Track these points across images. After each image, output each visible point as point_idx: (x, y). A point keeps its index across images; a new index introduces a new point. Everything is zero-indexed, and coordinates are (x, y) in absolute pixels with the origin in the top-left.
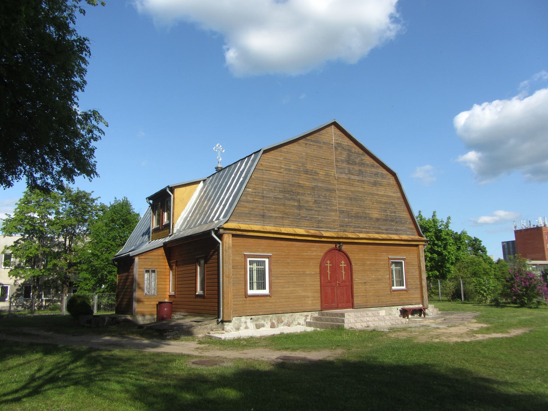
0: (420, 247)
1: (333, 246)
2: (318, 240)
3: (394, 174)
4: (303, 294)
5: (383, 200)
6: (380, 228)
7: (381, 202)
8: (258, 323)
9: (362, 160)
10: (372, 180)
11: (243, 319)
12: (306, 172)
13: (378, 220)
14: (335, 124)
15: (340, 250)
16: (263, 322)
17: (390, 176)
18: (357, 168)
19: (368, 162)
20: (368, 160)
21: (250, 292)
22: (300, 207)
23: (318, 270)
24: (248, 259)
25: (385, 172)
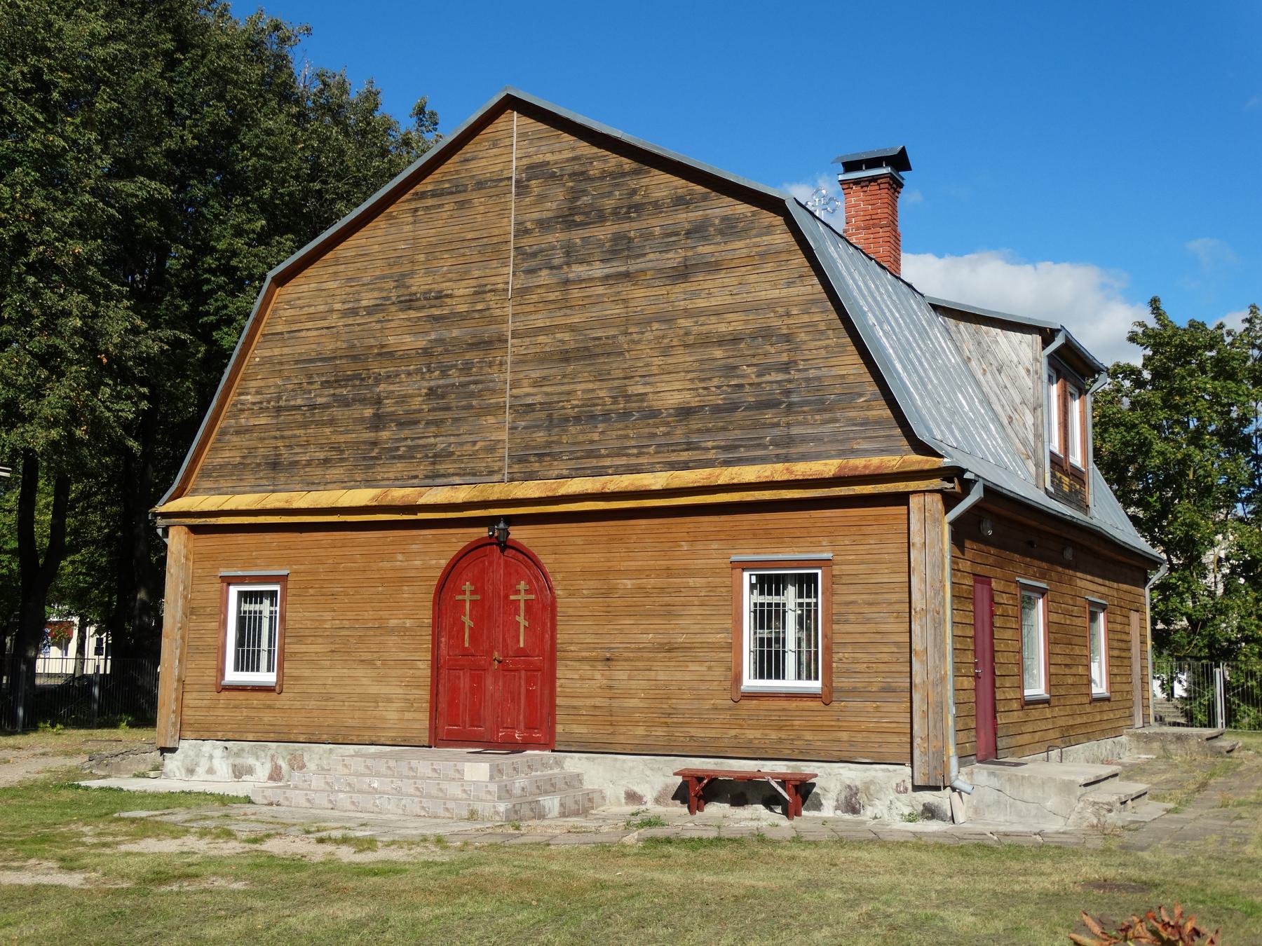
0: (914, 501)
1: (483, 532)
2: (408, 519)
3: (776, 205)
4: (374, 690)
5: (723, 328)
6: (690, 447)
7: (706, 341)
8: (238, 761)
9: (634, 192)
10: (674, 258)
11: (208, 746)
12: (409, 303)
13: (685, 413)
14: (511, 103)
15: (504, 545)
16: (251, 761)
17: (768, 218)
18: (603, 232)
19: (658, 194)
20: (662, 185)
21: (232, 676)
22: (378, 422)
23: (426, 616)
24: (233, 591)
25: (744, 209)
